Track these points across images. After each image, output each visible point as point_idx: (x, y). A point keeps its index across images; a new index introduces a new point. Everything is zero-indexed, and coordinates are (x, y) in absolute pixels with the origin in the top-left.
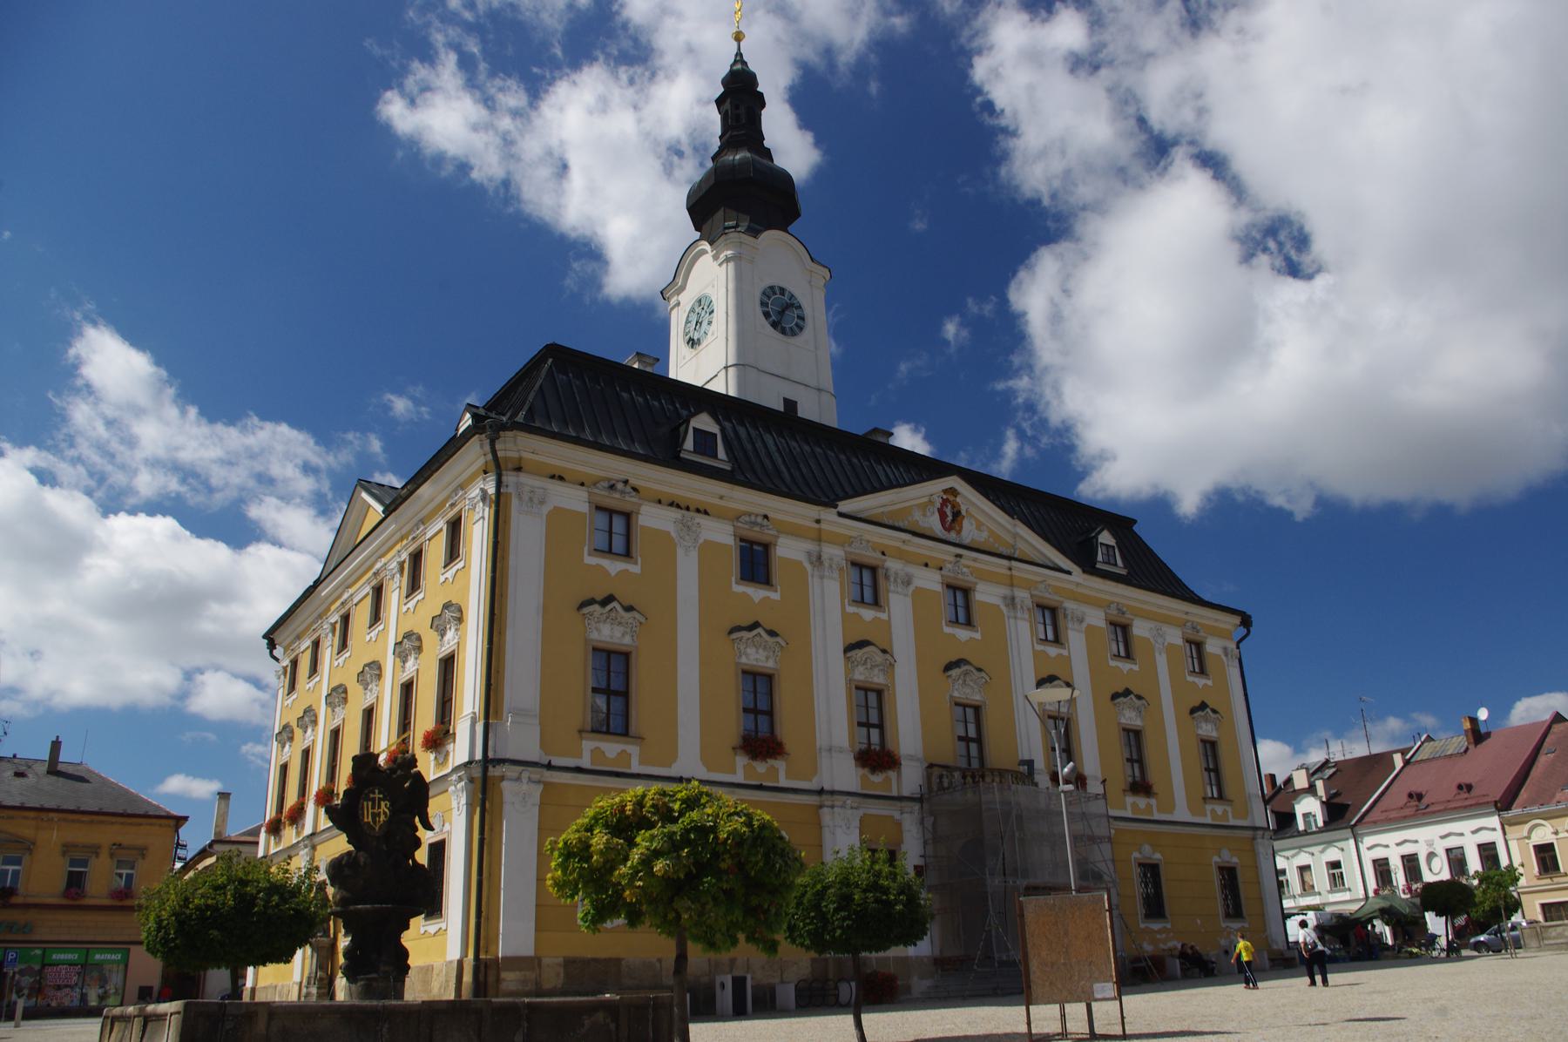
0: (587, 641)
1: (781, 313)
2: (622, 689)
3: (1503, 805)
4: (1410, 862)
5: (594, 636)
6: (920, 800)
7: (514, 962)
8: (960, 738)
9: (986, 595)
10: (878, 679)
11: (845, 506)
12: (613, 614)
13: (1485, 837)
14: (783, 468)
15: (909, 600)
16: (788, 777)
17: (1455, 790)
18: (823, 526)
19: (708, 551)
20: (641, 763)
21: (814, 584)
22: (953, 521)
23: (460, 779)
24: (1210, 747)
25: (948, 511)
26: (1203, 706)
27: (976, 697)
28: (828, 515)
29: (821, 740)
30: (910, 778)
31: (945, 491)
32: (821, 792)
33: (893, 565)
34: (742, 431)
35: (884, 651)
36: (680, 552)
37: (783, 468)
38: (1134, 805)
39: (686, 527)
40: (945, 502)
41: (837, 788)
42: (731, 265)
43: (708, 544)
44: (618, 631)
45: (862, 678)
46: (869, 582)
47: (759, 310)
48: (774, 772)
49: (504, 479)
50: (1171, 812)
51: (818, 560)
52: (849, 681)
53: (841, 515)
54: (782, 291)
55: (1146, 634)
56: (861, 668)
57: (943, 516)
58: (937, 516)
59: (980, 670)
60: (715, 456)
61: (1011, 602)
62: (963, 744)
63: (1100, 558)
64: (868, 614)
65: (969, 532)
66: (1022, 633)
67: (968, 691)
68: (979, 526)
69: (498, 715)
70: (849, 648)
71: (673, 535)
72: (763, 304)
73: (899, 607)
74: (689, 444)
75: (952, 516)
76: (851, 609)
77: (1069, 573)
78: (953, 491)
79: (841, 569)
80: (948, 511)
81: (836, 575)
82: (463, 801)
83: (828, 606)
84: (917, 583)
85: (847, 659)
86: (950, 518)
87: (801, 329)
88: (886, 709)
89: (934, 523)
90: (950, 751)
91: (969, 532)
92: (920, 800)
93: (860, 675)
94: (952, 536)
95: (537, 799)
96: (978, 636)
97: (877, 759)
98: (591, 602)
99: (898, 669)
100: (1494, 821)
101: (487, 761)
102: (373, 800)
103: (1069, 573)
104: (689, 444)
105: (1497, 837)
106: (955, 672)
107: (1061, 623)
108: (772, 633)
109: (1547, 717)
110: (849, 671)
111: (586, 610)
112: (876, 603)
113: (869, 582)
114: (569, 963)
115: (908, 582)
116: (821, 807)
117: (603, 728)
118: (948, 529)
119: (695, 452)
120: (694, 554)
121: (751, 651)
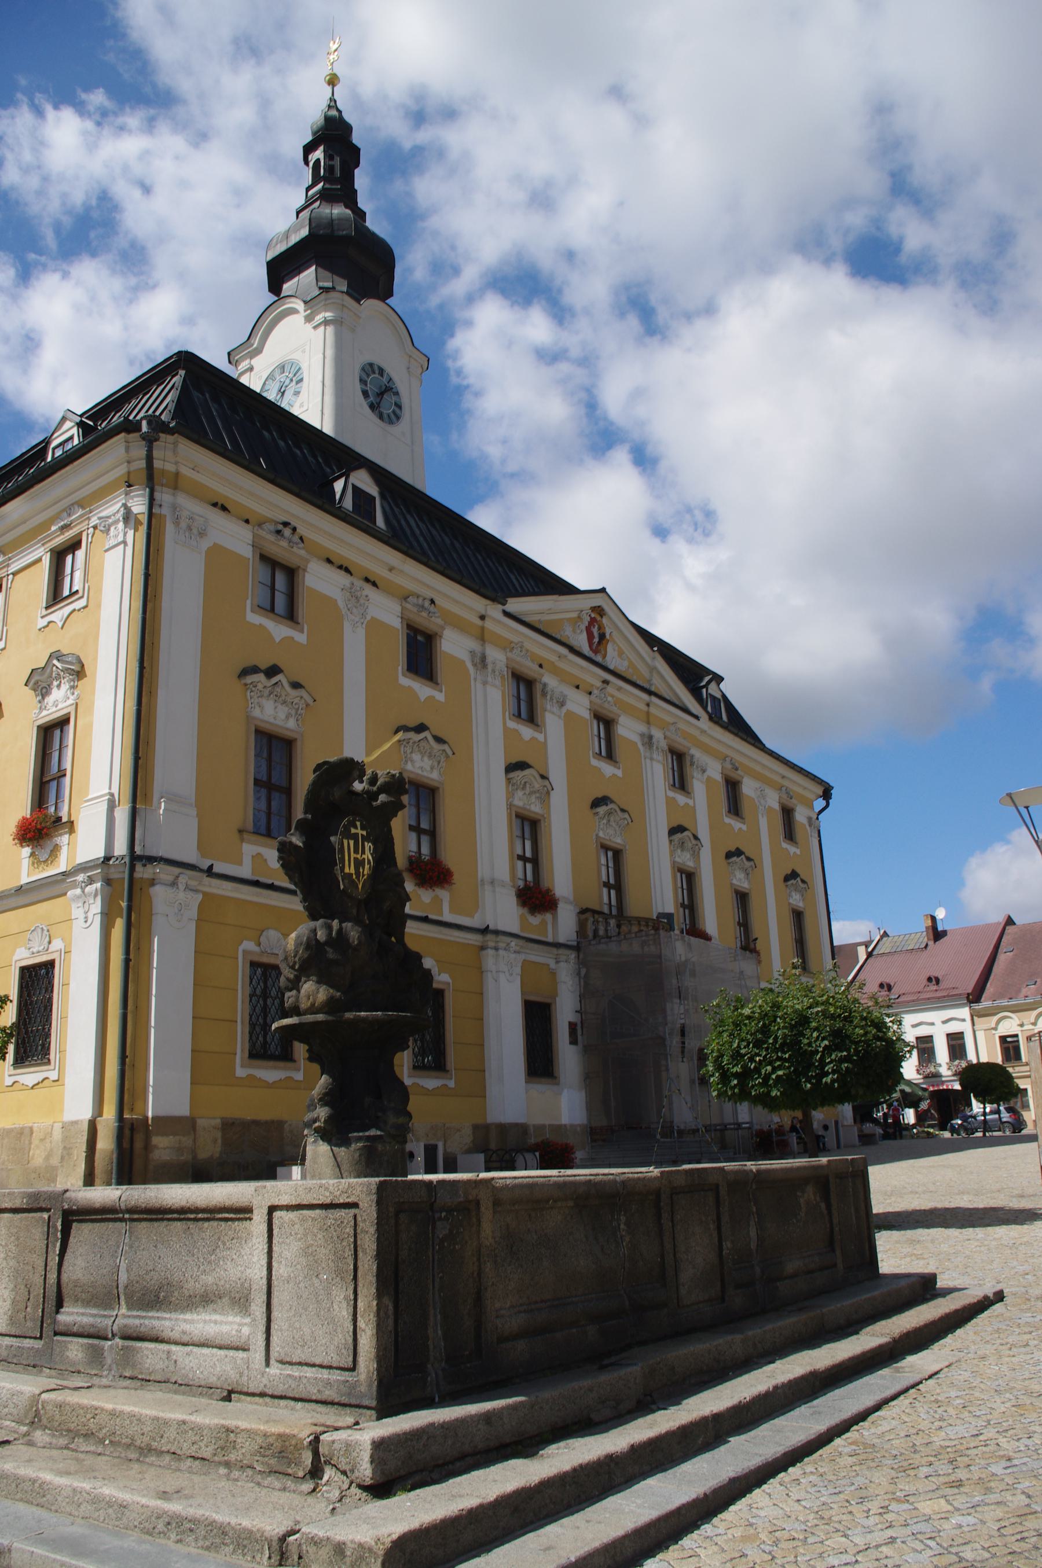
0: (249, 718)
1: (381, 395)
2: (284, 784)
3: (974, 997)
4: (956, 1044)
5: (257, 713)
6: (577, 948)
7: (166, 1124)
10: (535, 808)
12: (278, 689)
13: (954, 1027)
16: (452, 910)
17: (925, 982)
18: (488, 624)
21: (476, 688)
22: (599, 643)
23: (91, 881)
24: (798, 916)
25: (595, 631)
27: (617, 841)
29: (483, 871)
30: (565, 924)
31: (594, 609)
32: (485, 931)
35: (543, 777)
36: (347, 626)
39: (354, 596)
40: (593, 621)
41: (501, 928)
42: (330, 329)
44: (282, 712)
45: (521, 804)
46: (527, 697)
47: (358, 387)
48: (437, 902)
49: (157, 495)
51: (482, 662)
52: (510, 806)
53: (507, 614)
54: (381, 371)
57: (590, 637)
58: (585, 635)
59: (623, 810)
61: (648, 740)
68: (621, 653)
69: (147, 798)
70: (511, 768)
71: (341, 604)
72: (362, 381)
77: (697, 717)
81: (498, 682)
82: (96, 907)
84: (570, 706)
85: (509, 780)
86: (596, 640)
87: (398, 418)
88: (543, 842)
89: (581, 641)
92: (577, 948)
94: (598, 658)
95: (194, 913)
97: (536, 898)
98: (254, 670)
100: (964, 1012)
101: (134, 858)
102: (355, 837)
103: (697, 717)
105: (966, 1028)
106: (602, 810)
107: (688, 769)
108: (439, 740)
109: (1001, 919)
110: (510, 795)
111: (249, 679)
114: (228, 1125)
115: (562, 704)
116: (483, 948)
118: (596, 652)
120: (361, 632)
121: (416, 757)
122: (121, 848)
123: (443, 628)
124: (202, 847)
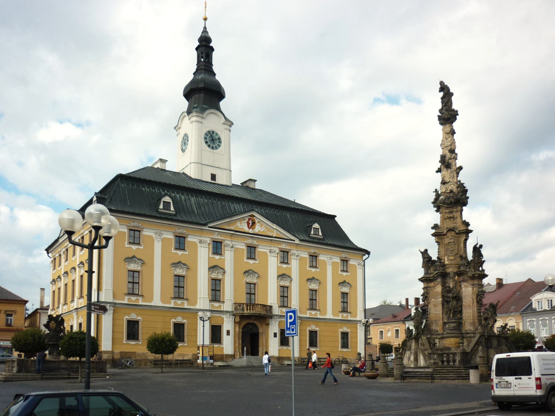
8: (247, 293)
10: (220, 277)
14: (195, 210)
15: (233, 253)
24: (344, 295)
28: (206, 228)
30: (228, 306)
31: (250, 216)
34: (183, 197)
36: (156, 242)
37: (195, 210)
38: (310, 313)
40: (249, 219)
44: (136, 266)
46: (217, 247)
53: (209, 227)
55: (325, 259)
56: (214, 274)
57: (248, 223)
60: (170, 210)
62: (249, 295)
63: (312, 233)
64: (217, 257)
65: (258, 229)
74: (161, 207)
77: (294, 241)
80: (250, 222)
83: (203, 255)
85: (209, 271)
86: (251, 224)
90: (243, 299)
91: (258, 229)
93: (214, 276)
94: (251, 231)
96: (257, 262)
99: (226, 274)
103: (294, 241)
104: (161, 207)
106: (246, 274)
113: (217, 247)
118: (249, 228)
120: (160, 242)
123: (188, 235)
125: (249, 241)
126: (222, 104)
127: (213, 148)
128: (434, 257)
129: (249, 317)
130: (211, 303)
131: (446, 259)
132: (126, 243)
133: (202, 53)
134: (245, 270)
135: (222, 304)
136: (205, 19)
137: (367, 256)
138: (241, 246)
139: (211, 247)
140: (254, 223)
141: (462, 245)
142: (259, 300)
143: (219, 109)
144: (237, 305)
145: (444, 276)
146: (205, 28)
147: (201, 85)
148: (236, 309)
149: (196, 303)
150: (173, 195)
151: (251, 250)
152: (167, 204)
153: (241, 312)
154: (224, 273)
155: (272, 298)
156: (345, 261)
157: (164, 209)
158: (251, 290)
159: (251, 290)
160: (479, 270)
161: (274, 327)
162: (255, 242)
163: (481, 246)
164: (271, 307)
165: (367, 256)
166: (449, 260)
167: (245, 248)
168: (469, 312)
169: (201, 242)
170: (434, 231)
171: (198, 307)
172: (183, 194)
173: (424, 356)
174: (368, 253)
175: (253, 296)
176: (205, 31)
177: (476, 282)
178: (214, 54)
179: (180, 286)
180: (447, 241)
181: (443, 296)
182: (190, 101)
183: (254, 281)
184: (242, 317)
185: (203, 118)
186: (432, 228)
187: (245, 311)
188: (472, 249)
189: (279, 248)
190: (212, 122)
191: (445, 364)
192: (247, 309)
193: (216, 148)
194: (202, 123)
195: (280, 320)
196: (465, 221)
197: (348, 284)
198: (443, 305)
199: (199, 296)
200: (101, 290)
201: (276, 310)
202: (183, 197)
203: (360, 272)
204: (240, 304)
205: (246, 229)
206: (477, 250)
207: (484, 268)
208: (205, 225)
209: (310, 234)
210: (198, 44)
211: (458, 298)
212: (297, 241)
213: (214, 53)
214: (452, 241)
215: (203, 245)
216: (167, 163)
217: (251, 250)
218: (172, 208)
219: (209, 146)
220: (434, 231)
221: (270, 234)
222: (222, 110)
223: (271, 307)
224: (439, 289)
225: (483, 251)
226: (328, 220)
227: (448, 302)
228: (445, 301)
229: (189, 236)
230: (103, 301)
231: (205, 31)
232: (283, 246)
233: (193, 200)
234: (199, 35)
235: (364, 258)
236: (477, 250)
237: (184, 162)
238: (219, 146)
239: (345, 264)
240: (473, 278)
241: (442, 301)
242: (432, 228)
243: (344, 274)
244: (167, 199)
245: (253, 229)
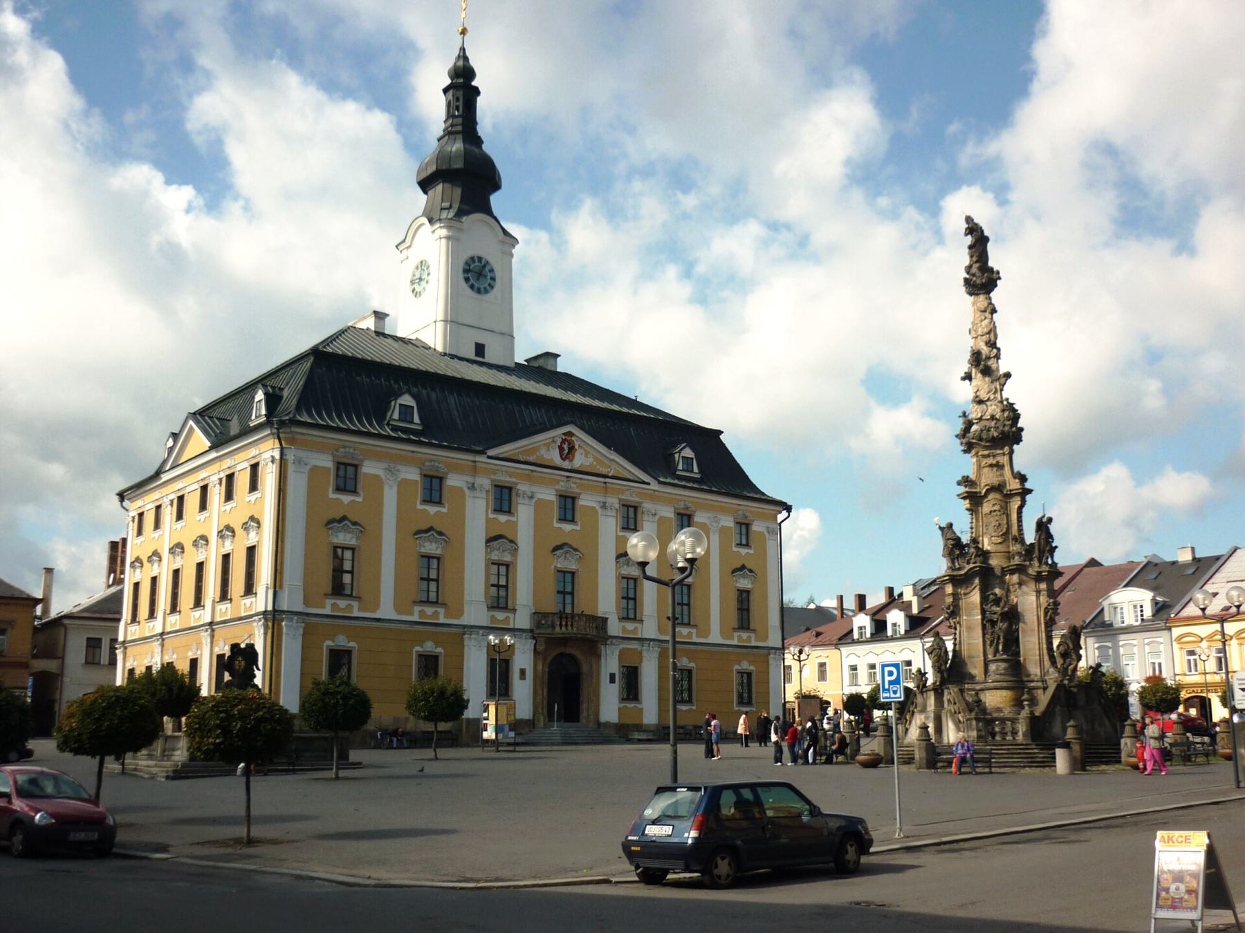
6: (531, 631)
8: (559, 592)
9: (587, 501)
10: (507, 558)
11: (491, 452)
15: (532, 508)
19: (403, 485)
20: (359, 610)
21: (469, 502)
25: (566, 447)
26: (743, 567)
27: (573, 567)
28: (482, 458)
30: (522, 619)
33: (523, 487)
35: (512, 541)
36: (386, 488)
39: (388, 470)
40: (563, 441)
43: (405, 481)
44: (349, 536)
46: (504, 499)
50: (707, 636)
51: (472, 487)
53: (489, 457)
55: (705, 521)
60: (412, 422)
63: (680, 467)
64: (503, 518)
65: (579, 460)
66: (609, 525)
67: (566, 562)
70: (489, 541)
73: (524, 515)
75: (568, 450)
76: (491, 516)
77: (648, 484)
78: (570, 434)
79: (487, 491)
80: (566, 447)
81: (484, 495)
83: (477, 515)
89: (555, 457)
90: (551, 604)
91: (579, 460)
93: (495, 556)
94: (566, 464)
96: (578, 528)
103: (648, 484)
104: (396, 416)
106: (558, 552)
112: (509, 512)
113: (504, 499)
117: (338, 590)
118: (563, 459)
119: (400, 420)
120: (395, 489)
121: (427, 544)
122: (270, 608)
124: (306, 602)
125: (562, 486)
126: (495, 200)
127: (479, 291)
128: (965, 539)
129: (564, 641)
130: (492, 613)
131: (986, 541)
132: (331, 490)
133: (458, 99)
134: (554, 545)
135: (511, 616)
136: (464, 32)
137: (785, 514)
138: (548, 495)
139: (491, 498)
140: (572, 449)
141: (1014, 517)
142: (582, 606)
143: (488, 211)
144: (540, 617)
145: (987, 576)
146: (463, 49)
147: (459, 165)
148: (539, 625)
149: (461, 613)
150: (415, 390)
151: (568, 506)
152: (406, 410)
153: (549, 631)
154: (516, 550)
155: (606, 602)
156: (744, 526)
157: (400, 420)
158: (567, 583)
159: (567, 583)
160: (1046, 563)
161: (611, 663)
162: (573, 488)
163: (1050, 520)
164: (605, 620)
165: (785, 514)
166: (991, 543)
167: (553, 498)
168: (1031, 644)
169: (472, 487)
170: (962, 489)
171: (465, 620)
172: (433, 389)
173: (958, 723)
174: (788, 509)
175: (568, 598)
176: (463, 56)
177: (1043, 586)
178: (480, 101)
179: (431, 577)
180: (986, 507)
181: (983, 612)
182: (430, 193)
183: (572, 566)
184: (552, 641)
185: (460, 230)
186: (959, 483)
187: (558, 629)
188: (1034, 526)
189: (620, 500)
190: (479, 238)
191: (998, 738)
192: (561, 626)
193: (486, 291)
194: (458, 240)
195: (622, 646)
196: (1019, 473)
197: (751, 571)
198: (984, 627)
199: (467, 597)
200: (281, 587)
201: (614, 628)
202: (433, 396)
203: (771, 546)
204: (545, 615)
205: (557, 460)
206: (1043, 526)
207: (1056, 560)
208: (482, 452)
209: (676, 469)
210: (448, 81)
211: (1013, 616)
212: (654, 485)
213: (479, 99)
214: (997, 507)
215: (478, 494)
216: (387, 319)
217: (568, 506)
218: (416, 419)
219: (472, 287)
220: (962, 489)
221: (603, 471)
222: (496, 213)
223: (605, 620)
224: (976, 597)
225: (1053, 528)
226: (708, 442)
227: (993, 623)
228: (988, 623)
229: (450, 476)
230: (285, 609)
231: (463, 56)
232: (629, 497)
233: (452, 400)
234: (450, 63)
235: (780, 517)
236: (1043, 526)
237: (421, 318)
238: (492, 287)
239: (744, 532)
240: (1038, 578)
241: (983, 619)
242: (959, 483)
243: (743, 551)
244: (407, 400)
245: (571, 461)
